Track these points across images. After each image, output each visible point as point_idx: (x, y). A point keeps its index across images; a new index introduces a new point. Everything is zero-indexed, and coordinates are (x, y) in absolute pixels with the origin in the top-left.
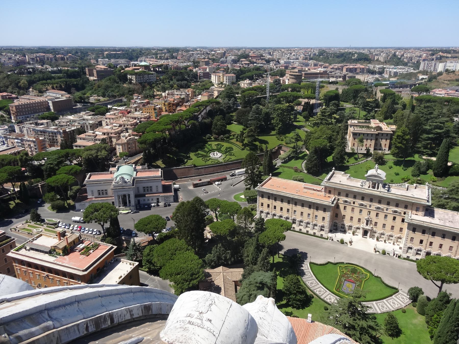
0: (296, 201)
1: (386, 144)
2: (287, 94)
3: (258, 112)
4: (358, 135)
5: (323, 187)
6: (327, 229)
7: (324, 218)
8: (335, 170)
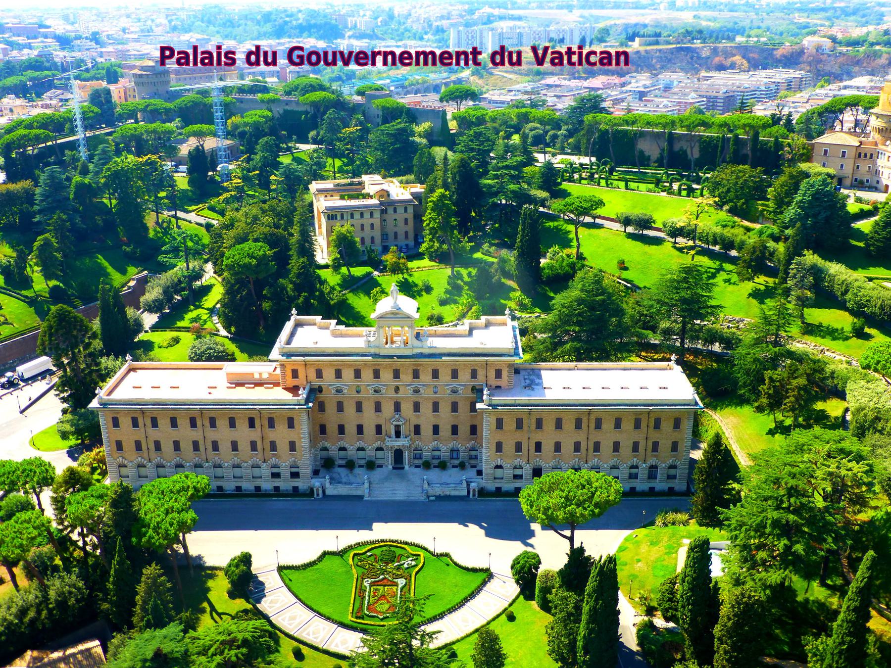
0: (213, 415)
1: (406, 233)
2: (135, 129)
4: (339, 217)
5: (274, 364)
6: (306, 470)
7: (292, 446)
8: (297, 315)
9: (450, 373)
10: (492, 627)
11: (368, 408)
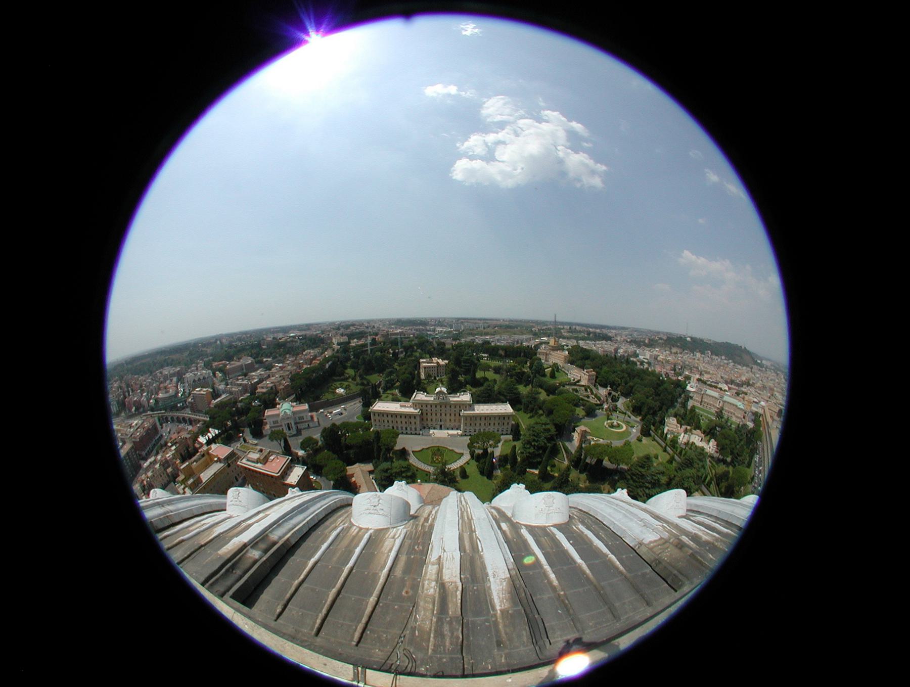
3: (364, 359)
10: (464, 466)
11: (434, 415)
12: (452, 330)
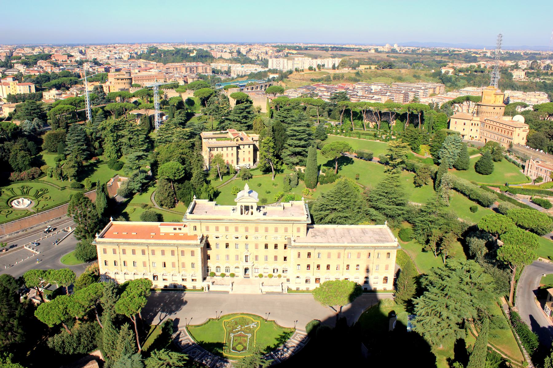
9: (274, 229)
12: (266, 69)
